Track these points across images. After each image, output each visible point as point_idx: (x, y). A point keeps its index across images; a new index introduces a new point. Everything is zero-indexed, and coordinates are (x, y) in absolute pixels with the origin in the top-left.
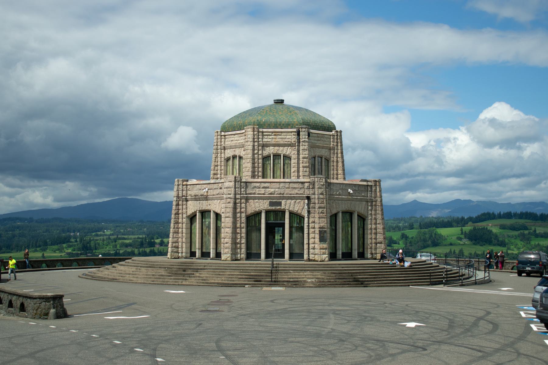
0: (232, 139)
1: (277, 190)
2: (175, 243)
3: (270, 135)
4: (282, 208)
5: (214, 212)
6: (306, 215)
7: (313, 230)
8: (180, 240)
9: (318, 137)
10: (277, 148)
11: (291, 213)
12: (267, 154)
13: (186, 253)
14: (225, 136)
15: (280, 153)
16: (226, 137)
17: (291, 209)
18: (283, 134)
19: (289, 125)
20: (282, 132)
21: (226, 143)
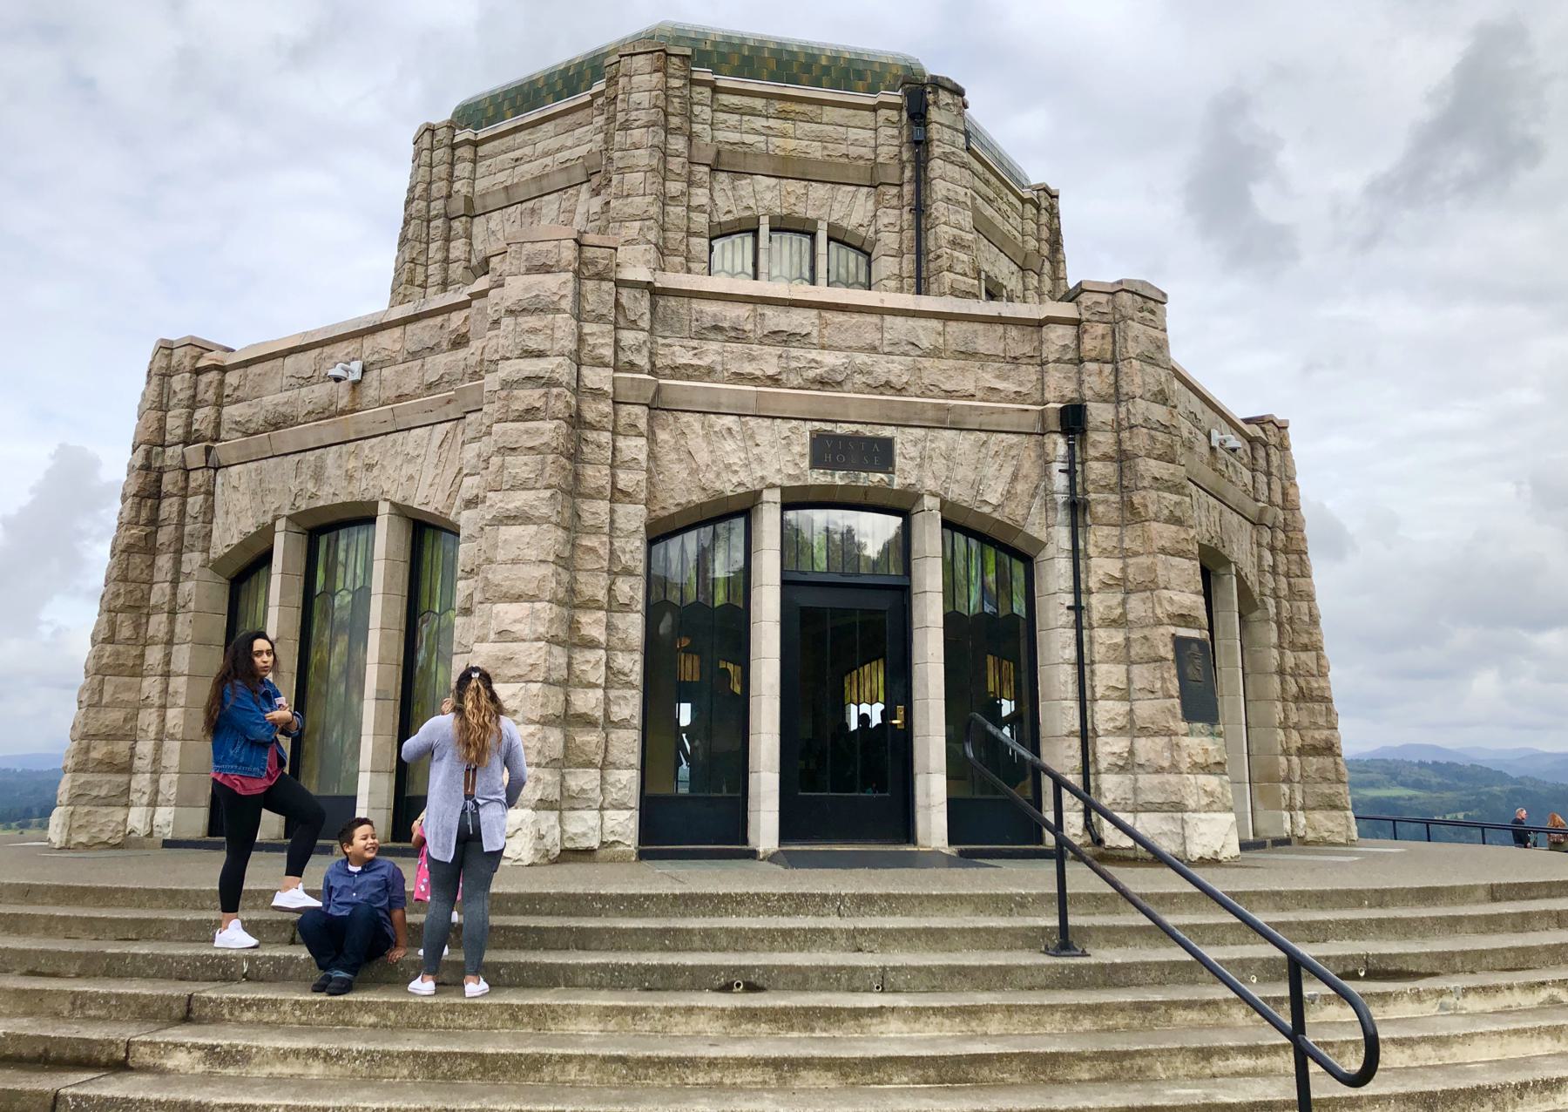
0: (517, 154)
1: (861, 358)
2: (110, 737)
3: (753, 113)
4: (898, 483)
5: (400, 510)
6: (1062, 536)
7: (1118, 637)
8: (148, 718)
9: (987, 183)
10: (797, 187)
11: (954, 522)
12: (738, 213)
13: (182, 802)
14: (476, 144)
15: (811, 214)
16: (482, 150)
17: (959, 493)
18: (830, 113)
19: (860, 75)
20: (821, 103)
21: (480, 185)
